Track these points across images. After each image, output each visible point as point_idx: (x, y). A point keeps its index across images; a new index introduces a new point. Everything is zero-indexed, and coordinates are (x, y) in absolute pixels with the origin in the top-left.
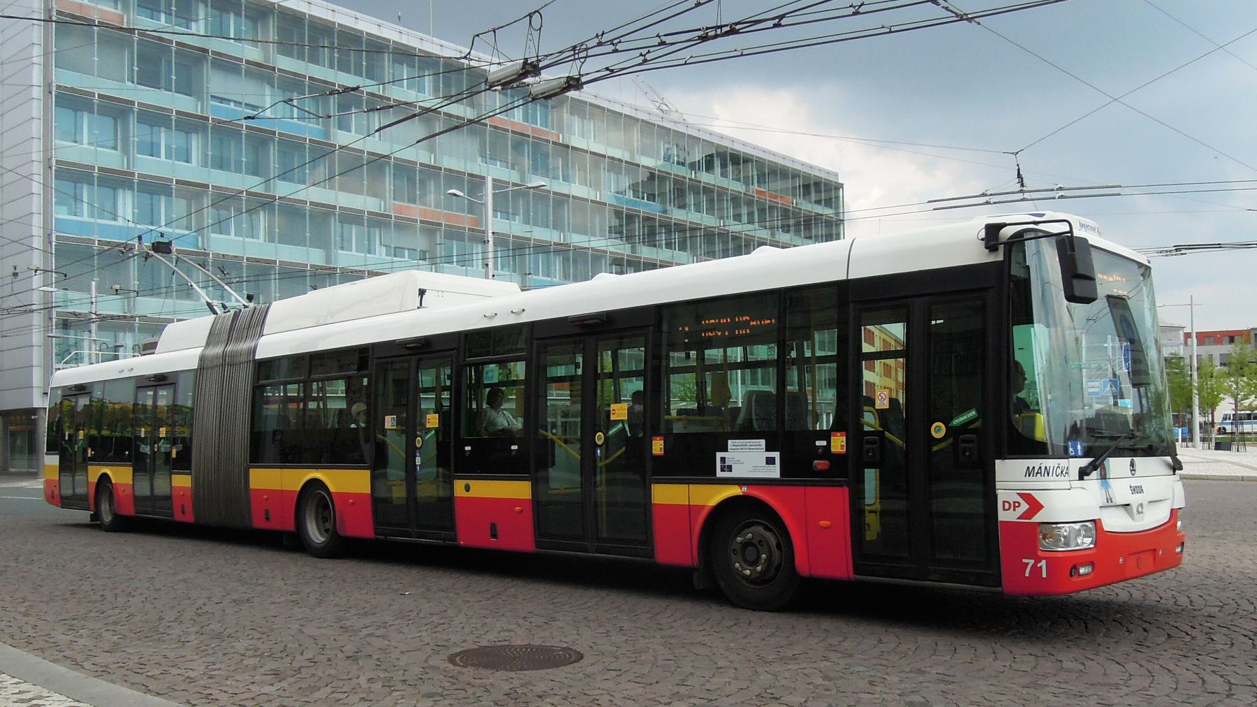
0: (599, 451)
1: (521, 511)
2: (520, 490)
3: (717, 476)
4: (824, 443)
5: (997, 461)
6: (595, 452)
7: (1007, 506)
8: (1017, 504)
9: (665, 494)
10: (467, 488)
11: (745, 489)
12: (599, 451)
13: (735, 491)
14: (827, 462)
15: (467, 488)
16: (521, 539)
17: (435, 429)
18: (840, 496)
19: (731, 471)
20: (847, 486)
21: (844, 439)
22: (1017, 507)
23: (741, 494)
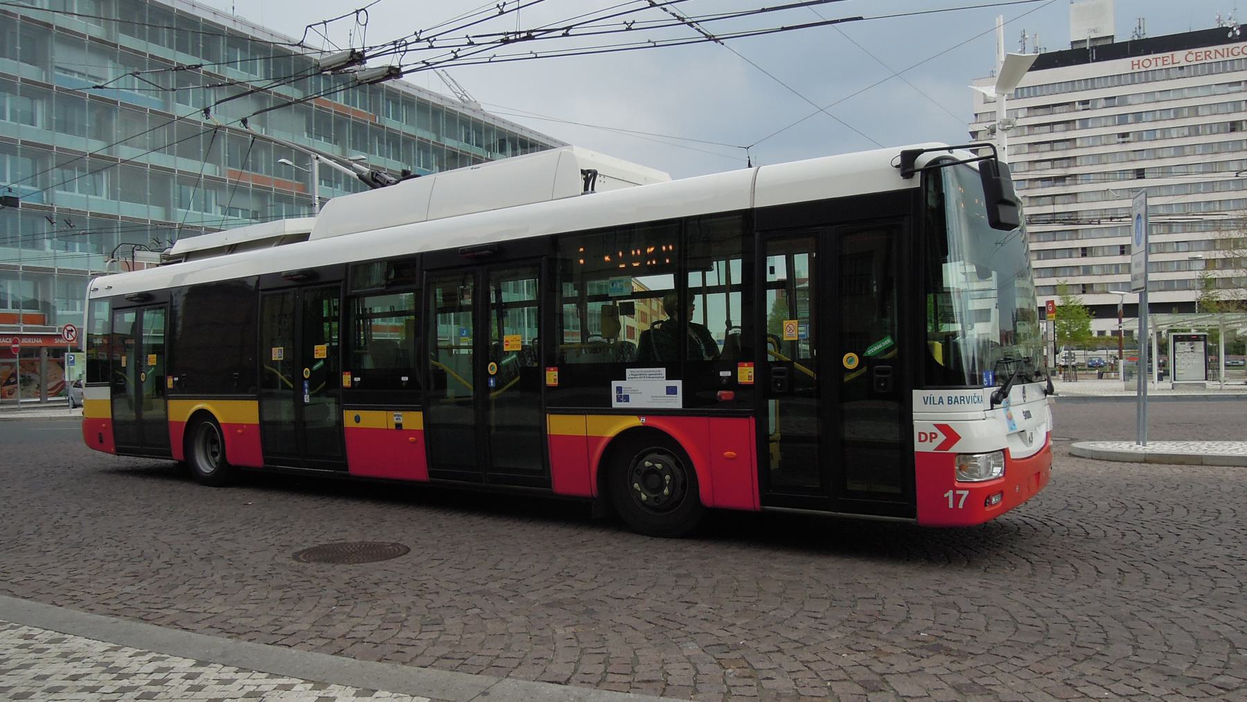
2: (413, 420)
3: (613, 406)
7: (923, 437)
8: (934, 436)
11: (643, 420)
13: (636, 421)
19: (628, 401)
20: (753, 417)
22: (934, 438)
23: (642, 425)
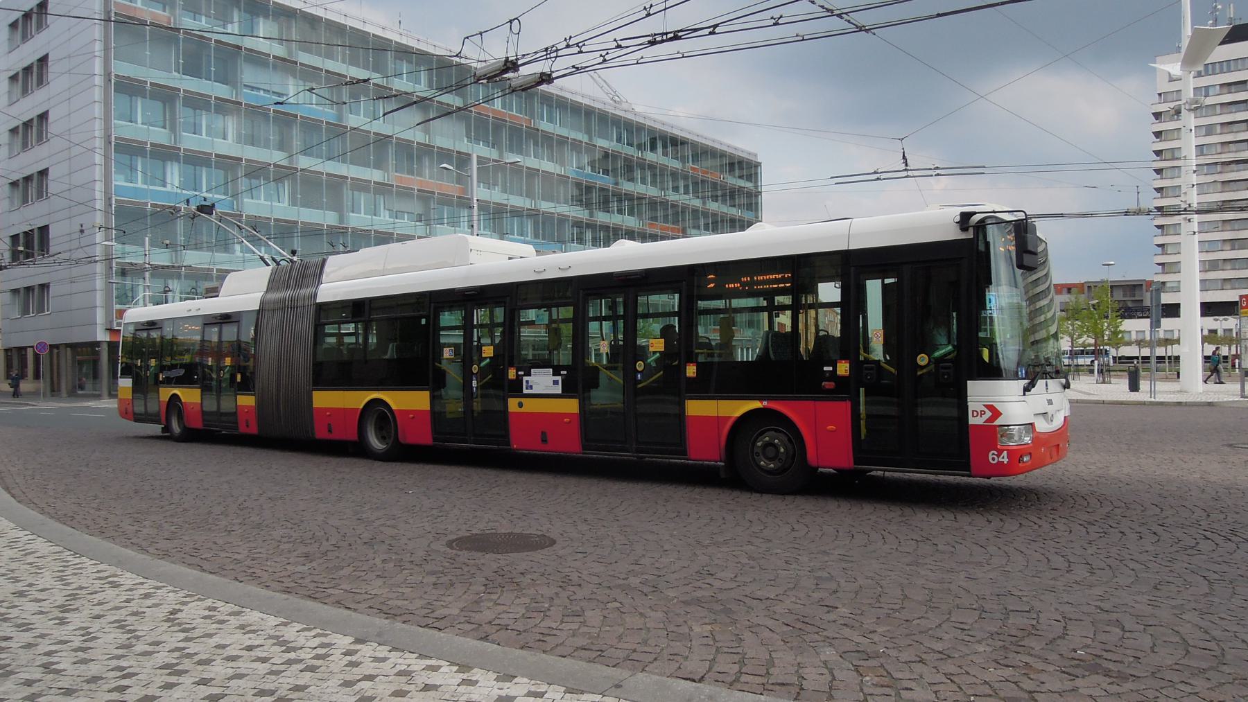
0: (639, 376)
1: (570, 422)
4: (831, 369)
5: (968, 382)
6: (636, 377)
9: (696, 408)
10: (520, 405)
11: (765, 403)
12: (639, 376)
14: (833, 383)
15: (520, 405)
16: (571, 445)
17: (490, 358)
18: (844, 407)
20: (849, 400)
21: (848, 365)
23: (762, 407)
